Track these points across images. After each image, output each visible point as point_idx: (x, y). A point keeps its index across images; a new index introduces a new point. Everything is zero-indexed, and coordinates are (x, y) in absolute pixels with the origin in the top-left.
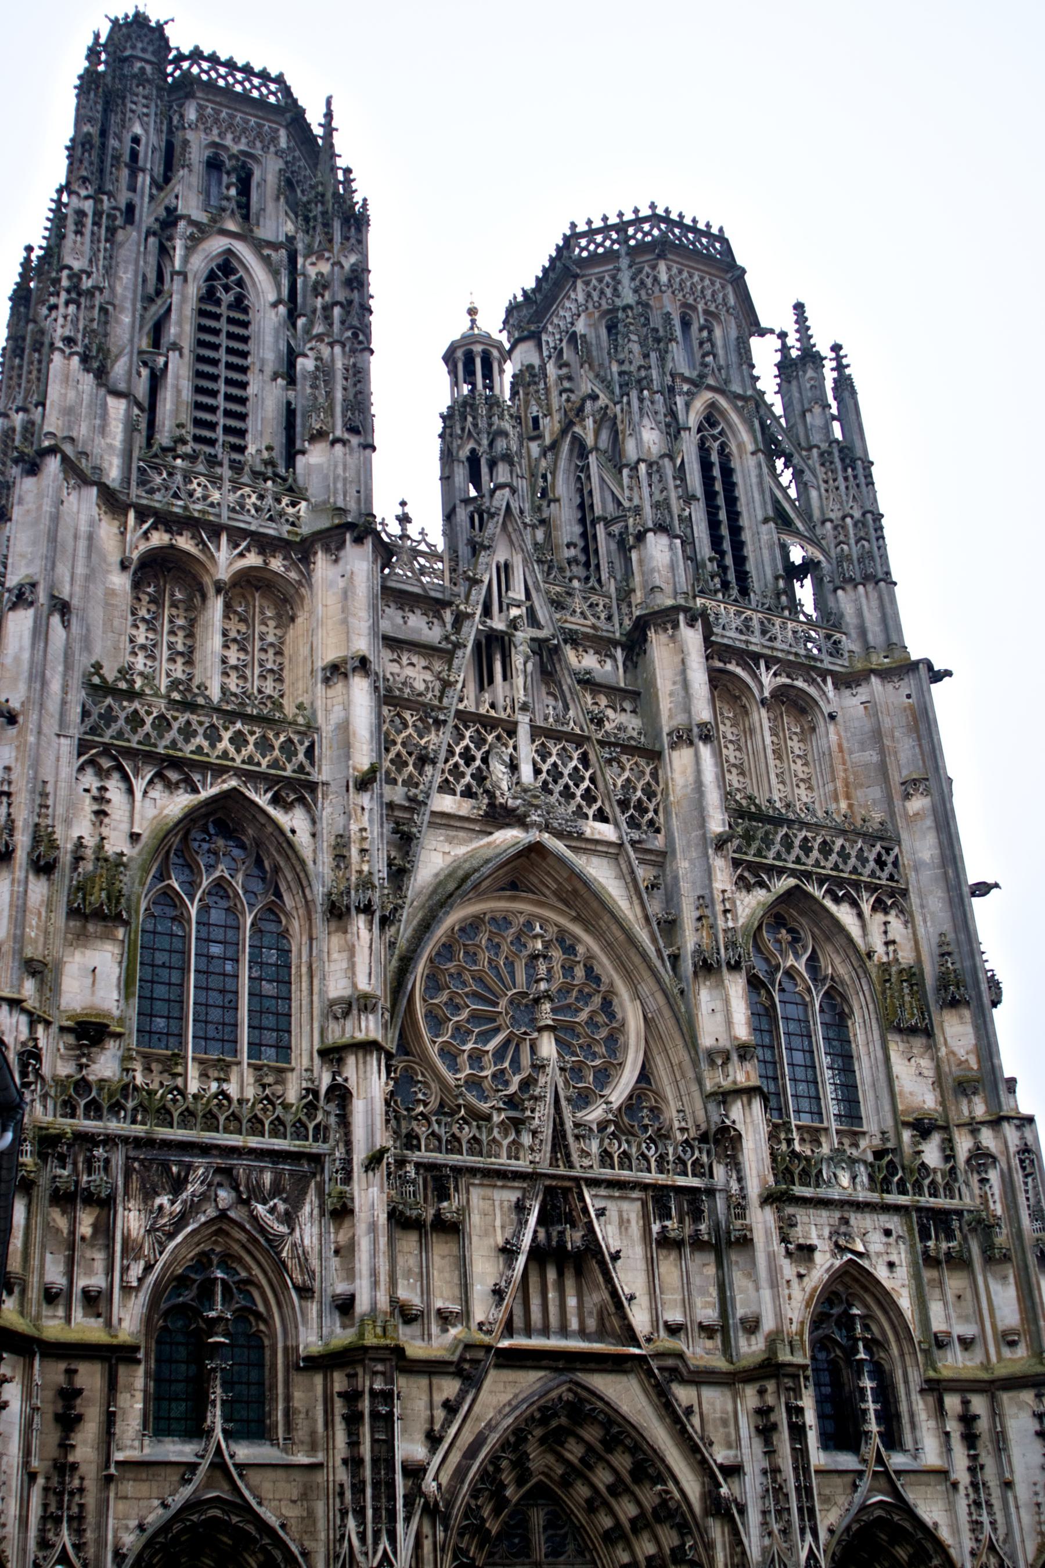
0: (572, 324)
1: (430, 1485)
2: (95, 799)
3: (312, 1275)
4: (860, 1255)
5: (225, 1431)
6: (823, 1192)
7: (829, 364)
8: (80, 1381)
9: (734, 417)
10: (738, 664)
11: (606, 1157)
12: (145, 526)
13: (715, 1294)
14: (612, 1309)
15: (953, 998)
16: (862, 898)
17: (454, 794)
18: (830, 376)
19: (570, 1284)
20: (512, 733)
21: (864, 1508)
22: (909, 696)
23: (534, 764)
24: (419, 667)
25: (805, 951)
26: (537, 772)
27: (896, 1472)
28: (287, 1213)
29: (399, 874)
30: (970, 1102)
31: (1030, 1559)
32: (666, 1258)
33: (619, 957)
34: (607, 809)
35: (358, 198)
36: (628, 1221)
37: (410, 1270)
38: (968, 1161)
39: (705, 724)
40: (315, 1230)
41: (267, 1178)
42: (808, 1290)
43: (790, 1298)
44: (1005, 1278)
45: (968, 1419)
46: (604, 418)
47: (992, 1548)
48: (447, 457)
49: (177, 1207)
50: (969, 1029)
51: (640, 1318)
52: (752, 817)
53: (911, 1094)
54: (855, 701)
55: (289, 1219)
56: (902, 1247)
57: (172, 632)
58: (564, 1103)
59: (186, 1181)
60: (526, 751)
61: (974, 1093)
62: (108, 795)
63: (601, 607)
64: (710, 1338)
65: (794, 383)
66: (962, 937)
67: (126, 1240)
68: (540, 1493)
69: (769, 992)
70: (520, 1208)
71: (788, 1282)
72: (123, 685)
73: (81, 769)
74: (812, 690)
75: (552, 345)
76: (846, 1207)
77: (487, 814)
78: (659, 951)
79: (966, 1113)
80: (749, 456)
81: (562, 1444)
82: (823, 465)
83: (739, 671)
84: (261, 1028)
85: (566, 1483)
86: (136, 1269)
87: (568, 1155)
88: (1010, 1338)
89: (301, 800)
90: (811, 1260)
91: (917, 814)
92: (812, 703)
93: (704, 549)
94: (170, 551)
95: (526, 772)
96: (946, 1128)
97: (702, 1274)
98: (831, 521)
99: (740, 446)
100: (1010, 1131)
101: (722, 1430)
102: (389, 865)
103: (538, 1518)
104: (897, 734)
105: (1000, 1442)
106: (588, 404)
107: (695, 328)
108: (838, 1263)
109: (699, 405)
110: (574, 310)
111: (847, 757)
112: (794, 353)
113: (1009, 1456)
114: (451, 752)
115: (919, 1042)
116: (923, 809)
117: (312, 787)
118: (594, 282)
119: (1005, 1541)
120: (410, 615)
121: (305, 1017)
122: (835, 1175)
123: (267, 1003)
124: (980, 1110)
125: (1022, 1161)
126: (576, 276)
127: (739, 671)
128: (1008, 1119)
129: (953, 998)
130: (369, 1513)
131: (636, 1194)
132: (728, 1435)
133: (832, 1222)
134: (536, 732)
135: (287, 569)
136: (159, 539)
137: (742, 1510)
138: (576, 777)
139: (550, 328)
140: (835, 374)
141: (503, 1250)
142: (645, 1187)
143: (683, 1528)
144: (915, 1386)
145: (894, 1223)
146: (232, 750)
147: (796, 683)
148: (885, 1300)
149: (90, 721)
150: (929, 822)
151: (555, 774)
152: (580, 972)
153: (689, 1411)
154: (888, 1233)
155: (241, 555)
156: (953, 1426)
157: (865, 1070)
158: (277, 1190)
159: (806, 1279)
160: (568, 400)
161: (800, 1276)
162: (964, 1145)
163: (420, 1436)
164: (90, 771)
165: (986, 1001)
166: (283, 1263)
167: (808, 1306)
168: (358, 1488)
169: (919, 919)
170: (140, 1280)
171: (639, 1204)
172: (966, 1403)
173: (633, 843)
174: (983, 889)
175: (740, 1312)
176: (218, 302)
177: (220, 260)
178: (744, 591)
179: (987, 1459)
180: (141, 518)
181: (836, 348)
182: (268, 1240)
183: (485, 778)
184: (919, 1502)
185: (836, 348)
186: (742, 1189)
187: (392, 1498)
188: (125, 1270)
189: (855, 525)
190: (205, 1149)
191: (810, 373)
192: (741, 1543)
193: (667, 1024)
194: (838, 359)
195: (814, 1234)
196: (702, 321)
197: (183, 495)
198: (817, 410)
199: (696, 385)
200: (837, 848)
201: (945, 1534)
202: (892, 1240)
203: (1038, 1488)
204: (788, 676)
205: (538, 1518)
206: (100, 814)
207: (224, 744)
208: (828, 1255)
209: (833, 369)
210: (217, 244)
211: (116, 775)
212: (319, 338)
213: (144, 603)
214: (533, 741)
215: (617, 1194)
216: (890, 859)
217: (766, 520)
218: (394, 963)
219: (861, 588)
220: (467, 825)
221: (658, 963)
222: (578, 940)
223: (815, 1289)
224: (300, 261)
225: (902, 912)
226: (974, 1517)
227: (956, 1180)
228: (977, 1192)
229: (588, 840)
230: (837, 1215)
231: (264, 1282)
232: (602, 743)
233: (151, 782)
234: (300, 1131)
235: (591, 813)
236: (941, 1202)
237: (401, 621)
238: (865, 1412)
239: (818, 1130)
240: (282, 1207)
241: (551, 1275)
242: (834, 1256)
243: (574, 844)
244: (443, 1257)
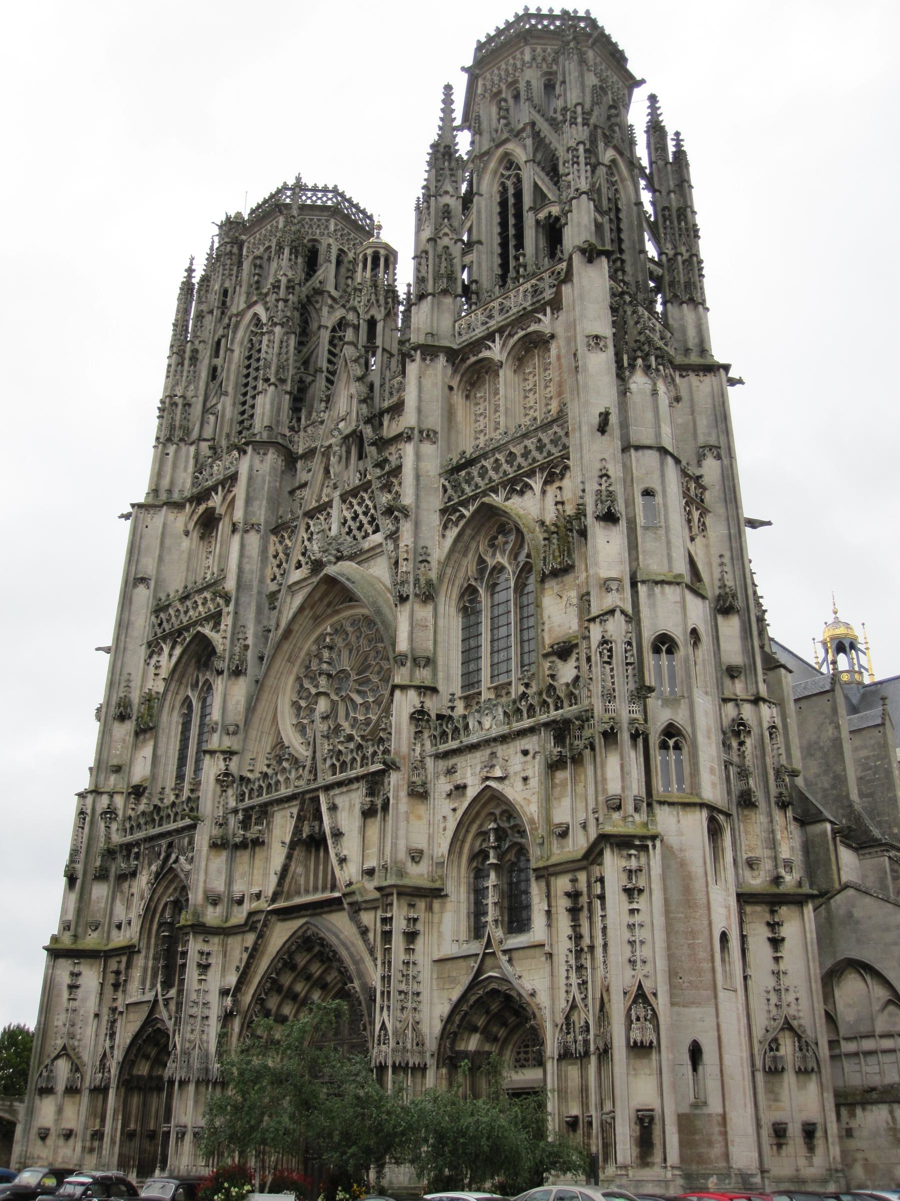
76: (492, 744)
90: (464, 795)
131: (355, 786)
142: (357, 779)
145: (530, 743)
154: (525, 753)
161: (454, 810)
184: (524, 974)
202: (529, 757)
214: (344, 501)
215: (345, 789)
230: (488, 751)
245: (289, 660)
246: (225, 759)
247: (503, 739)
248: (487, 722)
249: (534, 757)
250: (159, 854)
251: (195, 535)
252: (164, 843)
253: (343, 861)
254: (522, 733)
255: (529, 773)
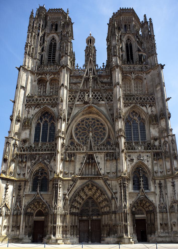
1: (67, 196)
2: (28, 111)
3: (52, 169)
4: (142, 160)
5: (39, 190)
6: (135, 151)
8: (21, 184)
10: (129, 74)
11: (98, 149)
12: (37, 75)
13: (116, 168)
14: (98, 171)
15: (162, 118)
16: (147, 105)
19: (93, 168)
20: (89, 91)
21: (139, 198)
22: (158, 71)
25: (138, 115)
27: (145, 193)
28: (49, 161)
30: (164, 134)
31: (169, 205)
32: (108, 163)
33: (105, 120)
34: (104, 99)
36: (102, 158)
37: (67, 167)
38: (163, 144)
41: (46, 157)
42: (132, 166)
43: (129, 167)
44: (168, 161)
45: (160, 184)
47: (162, 204)
49: (34, 162)
50: (165, 122)
51: (102, 172)
52: (128, 96)
53: (154, 134)
54: (149, 75)
55: (50, 162)
56: (150, 158)
57: (43, 89)
58: (92, 141)
59: (36, 158)
61: (165, 132)
62: (30, 111)
64: (114, 174)
66: (164, 108)
67: (28, 167)
68: (90, 198)
69: (130, 122)
70: (84, 157)
71: (129, 165)
72: (32, 96)
73: (26, 108)
74: (142, 76)
77: (84, 103)
78: (110, 118)
79: (163, 136)
81: (91, 190)
82: (147, 40)
83: (129, 75)
85: (93, 195)
86: (29, 170)
87: (92, 149)
88: (168, 171)
89: (55, 106)
90: (133, 161)
91: (158, 90)
92: (142, 78)
94: (42, 78)
95: (90, 96)
96: (160, 139)
97: (114, 164)
98: (147, 48)
100: (170, 138)
101: (115, 187)
103: (90, 201)
104: (156, 78)
105: (166, 187)
108: (137, 161)
109: (126, 37)
111: (148, 85)
113: (167, 190)
114: (79, 96)
115: (156, 126)
116: (159, 89)
117: (57, 104)
119: (165, 203)
122: (138, 148)
124: (166, 135)
125: (172, 142)
127: (129, 75)
128: (170, 135)
129: (162, 118)
132: (116, 188)
133: (137, 155)
135: (57, 76)
136: (40, 77)
137: (117, 199)
138: (99, 96)
141: (81, 164)
142: (104, 153)
143: (108, 202)
144: (151, 180)
145: (149, 154)
146: (46, 101)
147: (139, 75)
148: (147, 167)
149: (27, 102)
150: (160, 91)
151: (96, 96)
152: (100, 124)
153: (109, 185)
154: (148, 156)
155: (51, 76)
156: (157, 186)
157: (147, 132)
158: (48, 158)
159: (132, 164)
161: (131, 164)
162: (163, 141)
163: (67, 190)
164: (27, 108)
165: (167, 117)
166: (48, 168)
167: (132, 168)
169: (157, 107)
170: (29, 172)
171: (104, 155)
172: (160, 181)
173: (107, 103)
174: (168, 99)
175: (119, 169)
176: (52, 44)
177: (52, 38)
178: (133, 63)
179: (163, 190)
180: (37, 74)
182: (46, 165)
186: (119, 151)
188: (28, 170)
189: (151, 47)
190: (39, 154)
192: (116, 203)
193: (112, 129)
195: (134, 157)
197: (43, 70)
199: (125, 34)
200: (143, 98)
201: (154, 202)
202: (148, 157)
203: (171, 194)
204: (138, 74)
205: (90, 201)
206: (28, 113)
207: (45, 101)
208: (136, 160)
210: (51, 35)
211: (31, 108)
213: (40, 86)
214: (92, 91)
216: (153, 98)
217: (136, 51)
219: (151, 57)
220: (81, 105)
221: (110, 120)
222: (99, 119)
223: (133, 166)
225: (155, 106)
226: (160, 199)
227: (161, 147)
228: (165, 148)
229: (100, 104)
232: (103, 90)
233: (35, 108)
235: (101, 100)
236: (158, 151)
237: (76, 80)
238: (141, 184)
239: (138, 142)
240: (48, 160)
241: (90, 167)
242: (137, 160)
243: (98, 105)
244: (72, 165)
245: (75, 122)
246: (63, 140)
247: (142, 152)
248: (140, 148)
249: (149, 157)
250: (35, 159)
251: (36, 82)
252: (38, 156)
253: (101, 169)
254: (148, 152)
255: (149, 160)
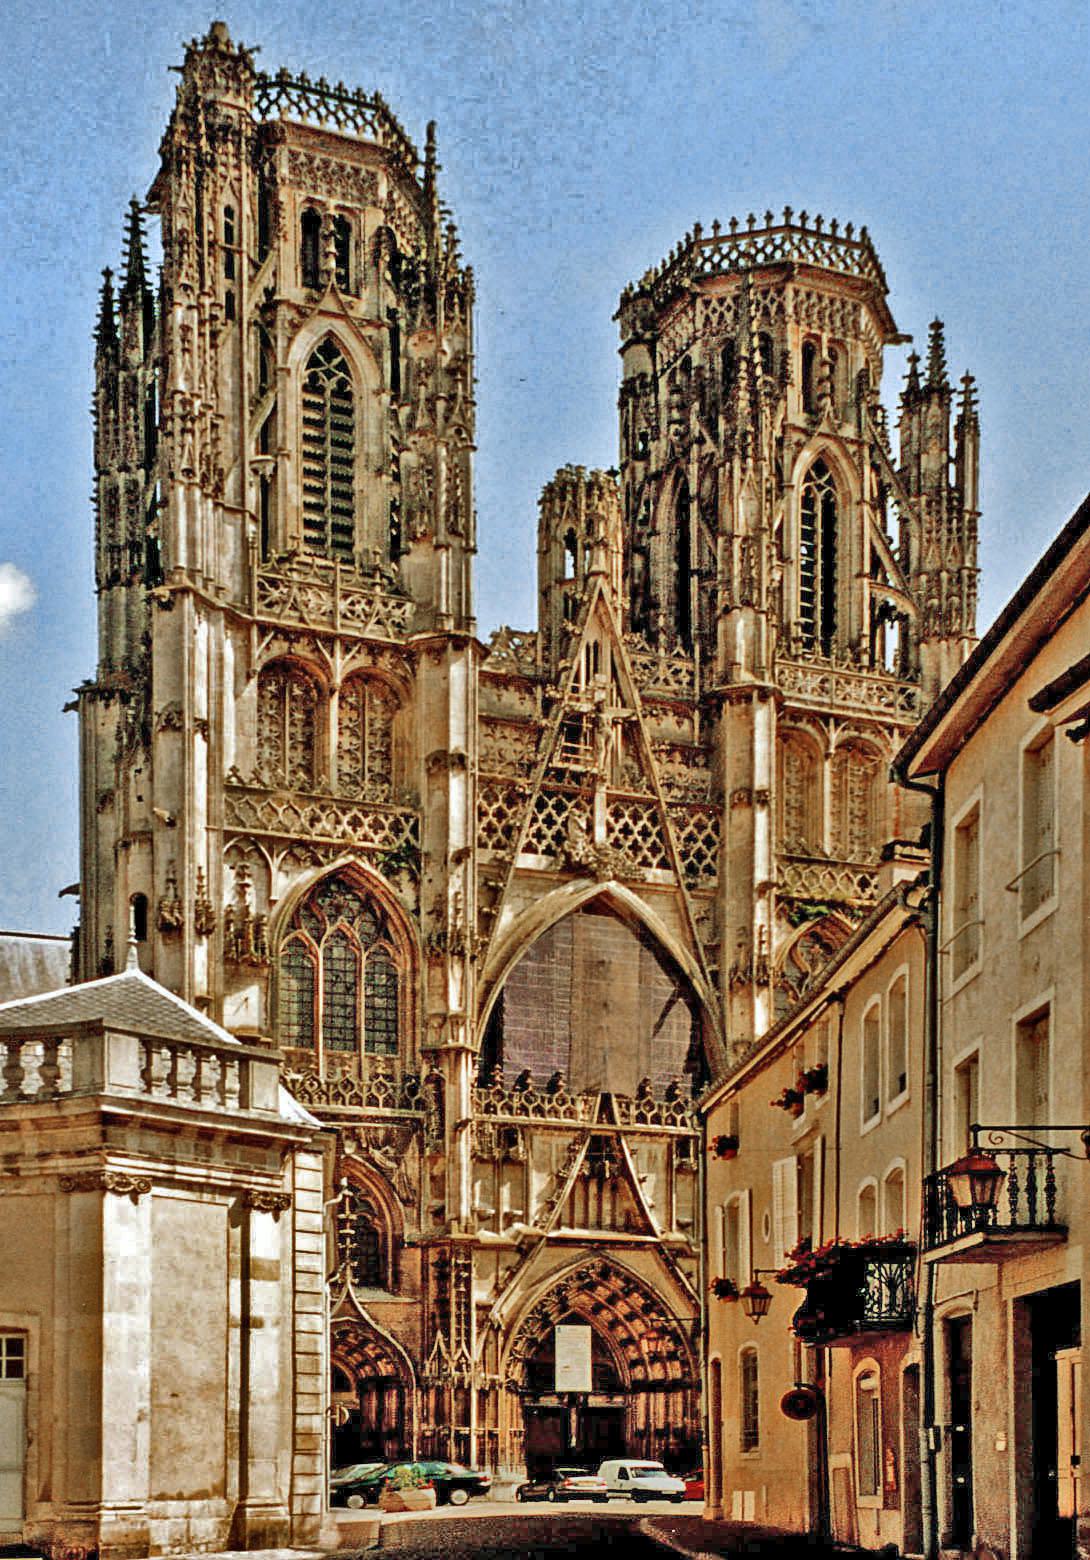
0: (688, 346)
7: (957, 399)
9: (844, 463)
17: (535, 851)
18: (956, 411)
20: (591, 801)
23: (608, 824)
24: (510, 740)
26: (610, 830)
29: (487, 921)
35: (462, 264)
39: (764, 791)
40: (417, 1166)
46: (708, 468)
48: (545, 528)
60: (602, 814)
63: (684, 673)
65: (915, 419)
75: (666, 360)
77: (563, 870)
80: (854, 507)
84: (374, 1030)
93: (794, 614)
95: (600, 832)
99: (847, 496)
102: (480, 912)
106: (695, 447)
107: (817, 360)
110: (691, 330)
112: (922, 383)
118: (714, 303)
120: (504, 692)
121: (409, 1024)
123: (378, 1013)
126: (695, 296)
130: (453, 1331)
134: (610, 799)
139: (665, 340)
140: (960, 411)
158: (388, 1140)
160: (677, 433)
168: (446, 1315)
181: (968, 379)
183: (565, 839)
185: (968, 379)
187: (468, 1323)
191: (934, 409)
194: (967, 392)
196: (825, 353)
198: (934, 451)
209: (959, 405)
212: (422, 432)
214: (608, 805)
218: (481, 985)
224: (402, 338)
231: (378, 1195)
234: (406, 1104)
237: (495, 698)
